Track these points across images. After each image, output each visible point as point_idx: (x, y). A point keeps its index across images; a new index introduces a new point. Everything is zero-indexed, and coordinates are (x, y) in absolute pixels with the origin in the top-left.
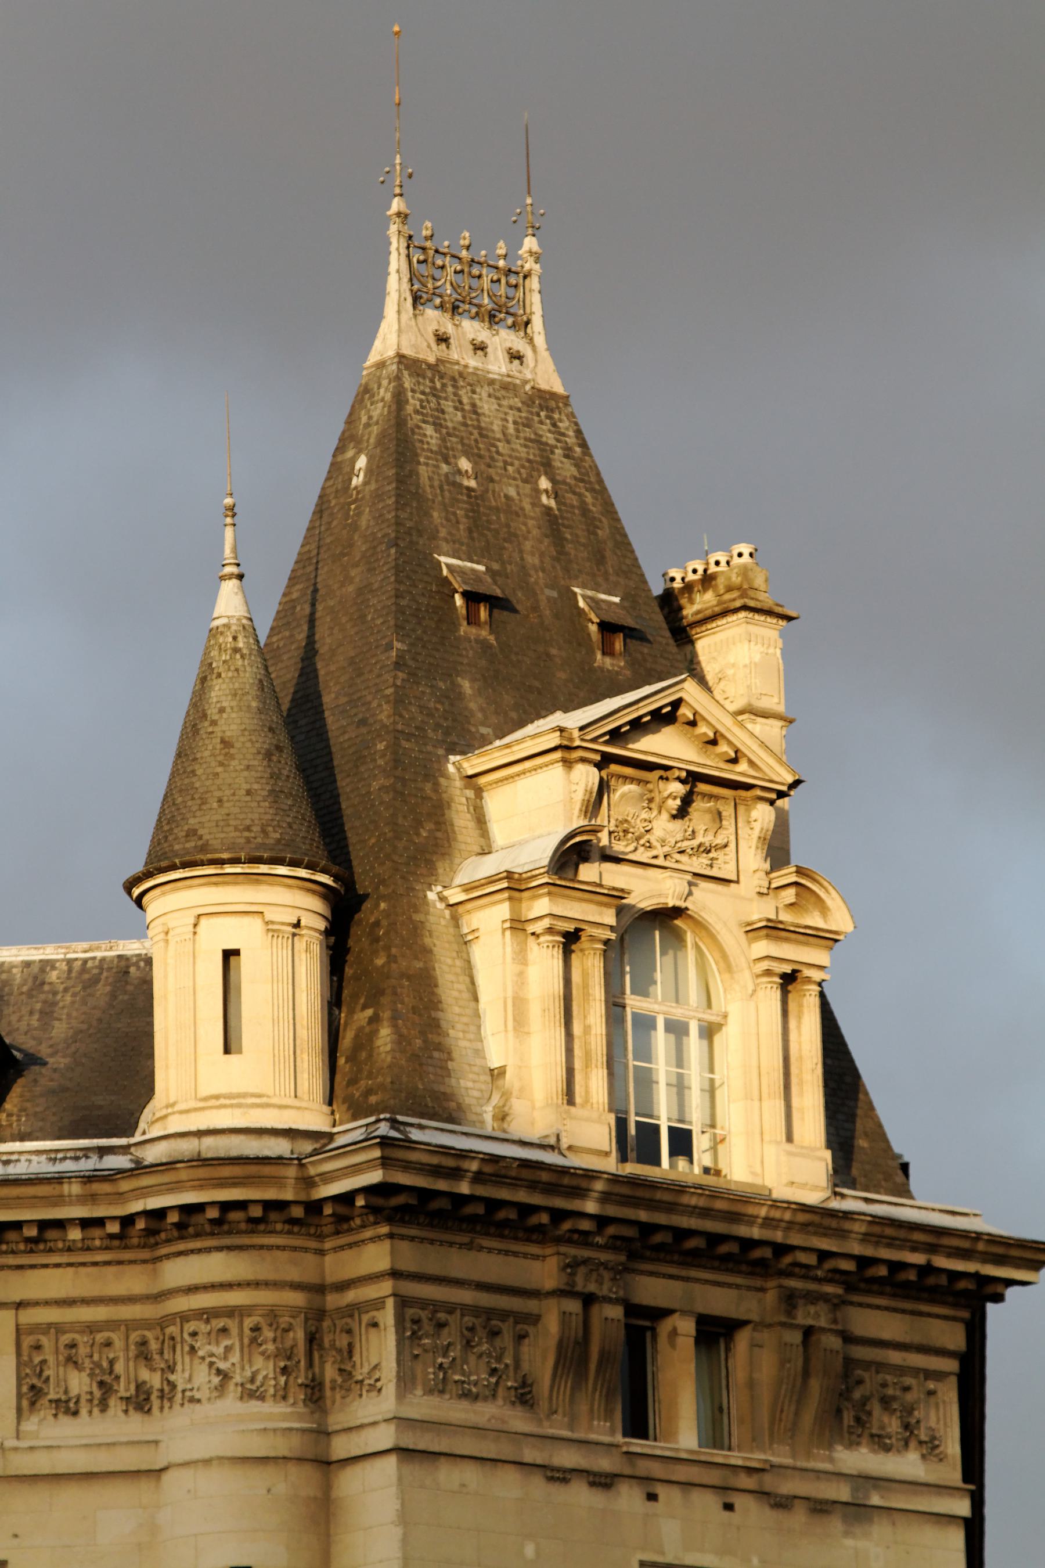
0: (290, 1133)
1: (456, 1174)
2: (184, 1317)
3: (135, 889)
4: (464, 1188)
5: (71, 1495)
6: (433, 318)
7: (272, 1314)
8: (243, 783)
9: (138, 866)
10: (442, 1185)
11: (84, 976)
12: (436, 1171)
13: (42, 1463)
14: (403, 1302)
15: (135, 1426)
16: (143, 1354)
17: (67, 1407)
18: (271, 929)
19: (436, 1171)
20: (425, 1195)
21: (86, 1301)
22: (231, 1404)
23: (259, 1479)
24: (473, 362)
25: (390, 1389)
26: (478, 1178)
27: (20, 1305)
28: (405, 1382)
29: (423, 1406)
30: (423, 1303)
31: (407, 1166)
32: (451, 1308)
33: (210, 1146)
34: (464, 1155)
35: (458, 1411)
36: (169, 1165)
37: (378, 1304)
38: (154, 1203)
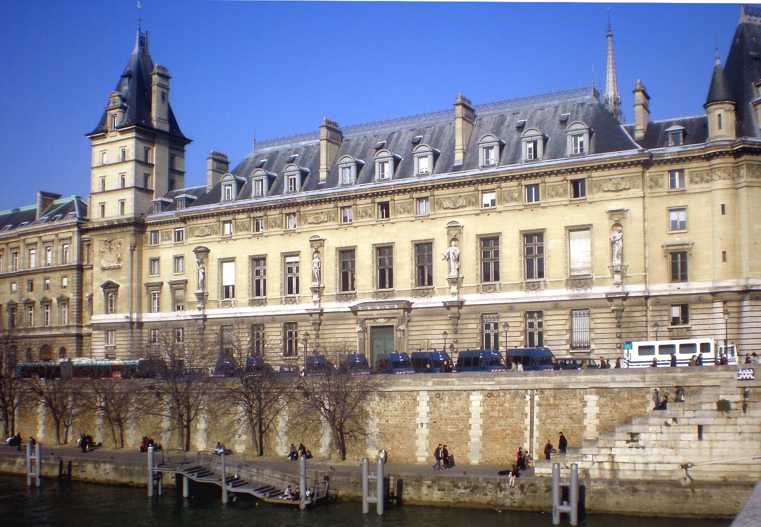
0: (729, 141)
1: (754, 145)
2: (714, 169)
3: (705, 106)
4: (756, 147)
5: (697, 195)
6: (748, 16)
7: (727, 167)
8: (721, 91)
9: (705, 103)
10: (752, 147)
11: (698, 120)
12: (752, 145)
13: (693, 191)
14: (747, 164)
15: (707, 185)
16: (708, 175)
17: (696, 183)
18: (726, 111)
19: (752, 145)
20: (750, 149)
21: (701, 167)
22: (721, 181)
23: (726, 192)
24: (755, 23)
25: (745, 177)
26: (758, 145)
27: (689, 169)
28: (747, 176)
29: (750, 179)
30: (750, 164)
31: (747, 144)
32: (754, 165)
33: (717, 143)
34: (756, 142)
35: (756, 180)
36: (711, 147)
37: (743, 165)
38: (709, 152)
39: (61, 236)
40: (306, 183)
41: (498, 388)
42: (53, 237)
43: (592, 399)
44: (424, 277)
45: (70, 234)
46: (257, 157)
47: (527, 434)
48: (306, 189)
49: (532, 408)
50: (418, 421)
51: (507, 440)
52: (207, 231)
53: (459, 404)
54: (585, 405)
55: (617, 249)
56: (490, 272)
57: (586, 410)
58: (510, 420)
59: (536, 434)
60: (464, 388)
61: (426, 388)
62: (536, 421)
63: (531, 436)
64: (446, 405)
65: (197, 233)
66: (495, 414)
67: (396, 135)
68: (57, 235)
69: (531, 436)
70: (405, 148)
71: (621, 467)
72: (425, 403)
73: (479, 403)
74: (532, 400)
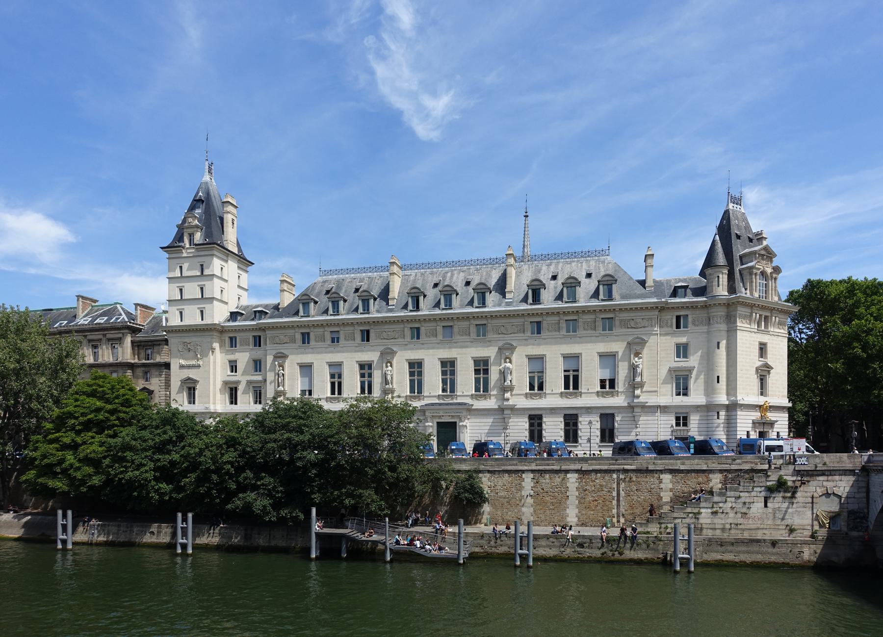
39: (108, 336)
40: (376, 306)
41: (591, 468)
42: (101, 337)
43: (667, 478)
44: (482, 386)
45: (120, 335)
46: (324, 282)
47: (615, 502)
48: (378, 311)
49: (618, 484)
50: (523, 493)
51: (599, 508)
52: (286, 339)
53: (557, 479)
54: (661, 482)
55: (639, 370)
56: (537, 385)
57: (662, 486)
58: (599, 494)
59: (622, 503)
60: (563, 468)
61: (530, 468)
62: (622, 493)
63: (618, 505)
64: (548, 481)
65: (277, 340)
66: (588, 487)
67: (449, 274)
68: (105, 335)
69: (618, 505)
70: (460, 285)
71: (704, 526)
72: (530, 480)
73: (574, 480)
74: (618, 477)
